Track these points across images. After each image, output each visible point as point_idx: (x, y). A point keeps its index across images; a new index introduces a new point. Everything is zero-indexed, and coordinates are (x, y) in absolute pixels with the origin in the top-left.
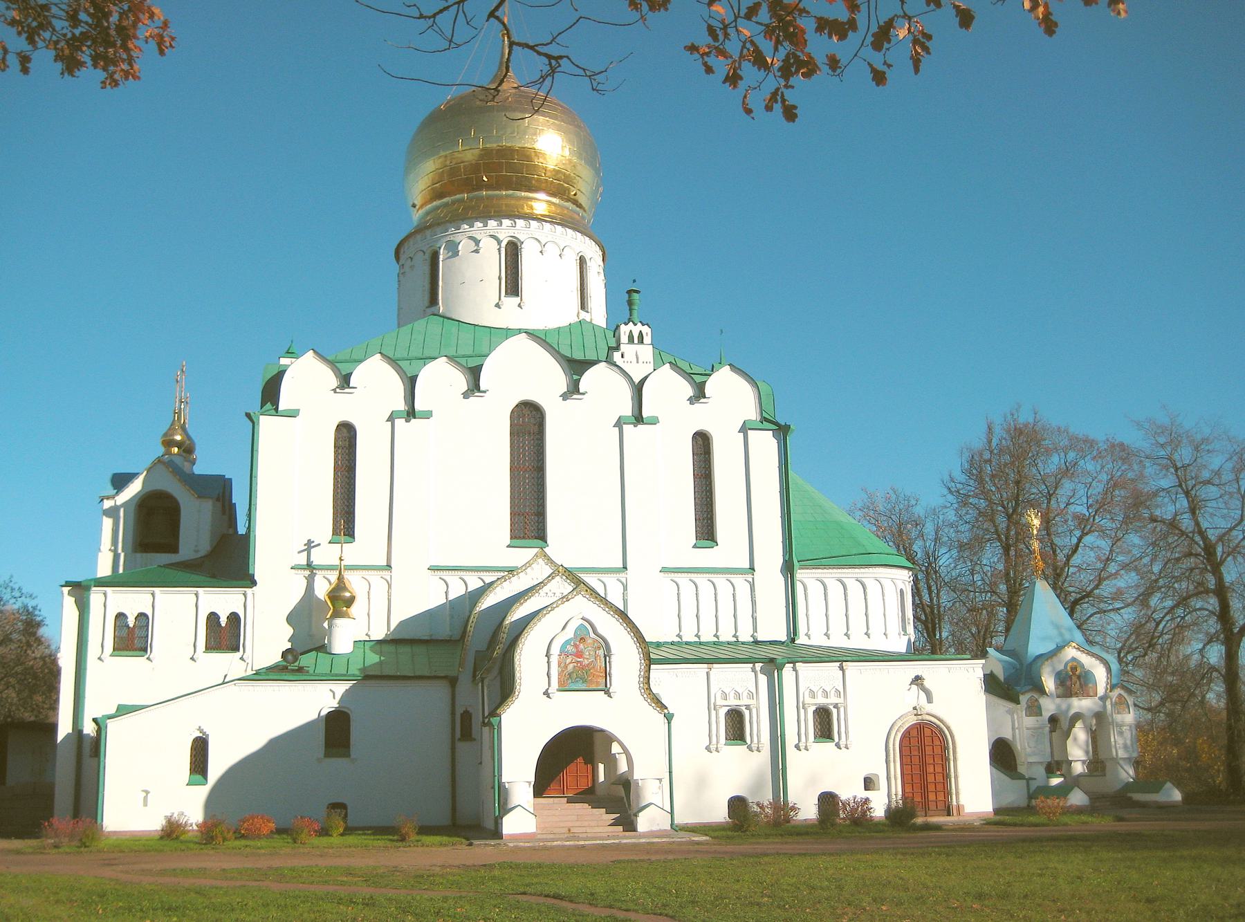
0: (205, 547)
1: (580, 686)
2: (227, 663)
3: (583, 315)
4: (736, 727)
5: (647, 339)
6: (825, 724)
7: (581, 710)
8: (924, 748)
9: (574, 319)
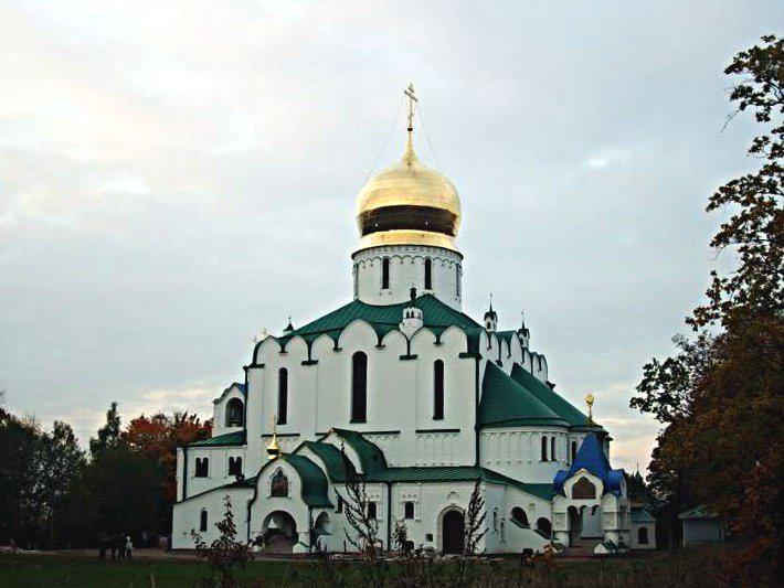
2: (233, 479)
5: (416, 315)
6: (409, 510)
7: (279, 504)
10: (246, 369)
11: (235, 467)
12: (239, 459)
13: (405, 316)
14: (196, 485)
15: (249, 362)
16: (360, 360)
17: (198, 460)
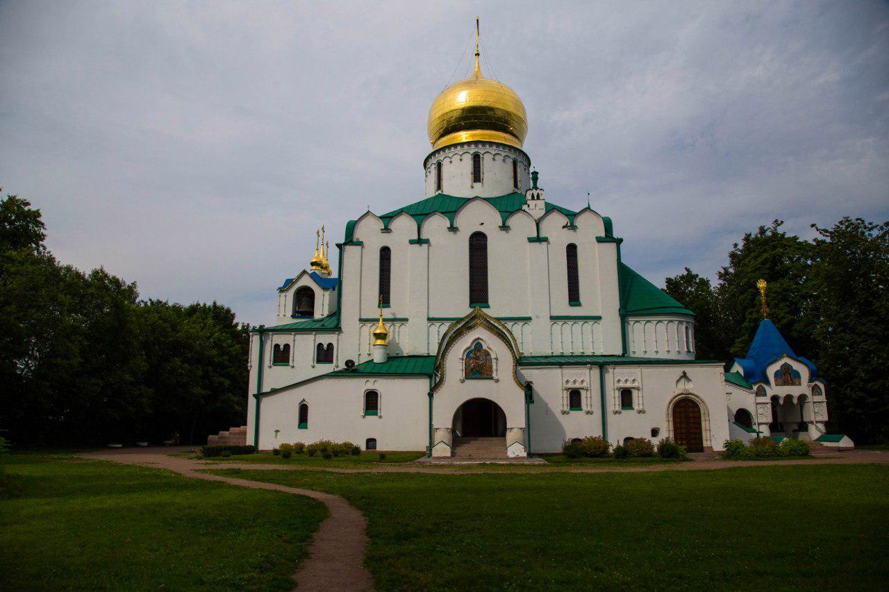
0: (326, 313)
1: (479, 376)
2: (326, 368)
3: (516, 190)
4: (575, 398)
6: (626, 397)
7: (479, 389)
8: (687, 413)
9: (510, 191)
10: (339, 246)
11: (324, 354)
12: (330, 345)
13: (529, 197)
14: (276, 376)
15: (342, 241)
16: (478, 243)
17: (277, 346)
